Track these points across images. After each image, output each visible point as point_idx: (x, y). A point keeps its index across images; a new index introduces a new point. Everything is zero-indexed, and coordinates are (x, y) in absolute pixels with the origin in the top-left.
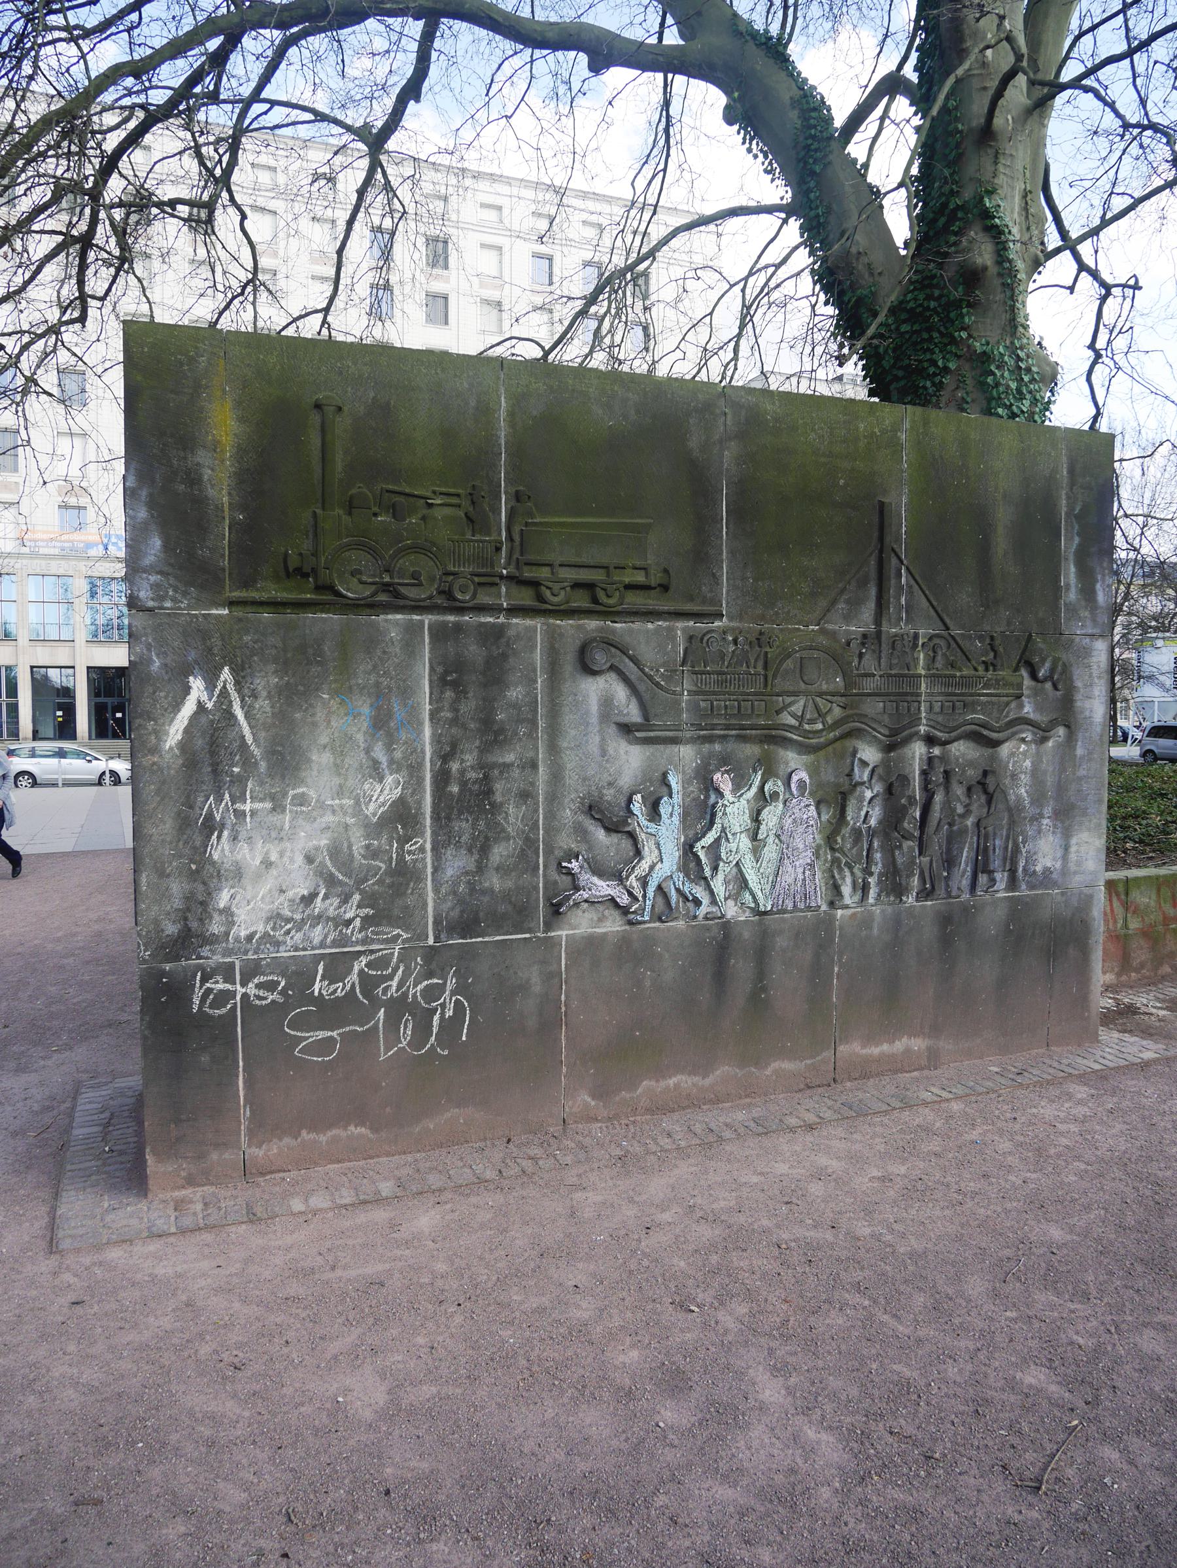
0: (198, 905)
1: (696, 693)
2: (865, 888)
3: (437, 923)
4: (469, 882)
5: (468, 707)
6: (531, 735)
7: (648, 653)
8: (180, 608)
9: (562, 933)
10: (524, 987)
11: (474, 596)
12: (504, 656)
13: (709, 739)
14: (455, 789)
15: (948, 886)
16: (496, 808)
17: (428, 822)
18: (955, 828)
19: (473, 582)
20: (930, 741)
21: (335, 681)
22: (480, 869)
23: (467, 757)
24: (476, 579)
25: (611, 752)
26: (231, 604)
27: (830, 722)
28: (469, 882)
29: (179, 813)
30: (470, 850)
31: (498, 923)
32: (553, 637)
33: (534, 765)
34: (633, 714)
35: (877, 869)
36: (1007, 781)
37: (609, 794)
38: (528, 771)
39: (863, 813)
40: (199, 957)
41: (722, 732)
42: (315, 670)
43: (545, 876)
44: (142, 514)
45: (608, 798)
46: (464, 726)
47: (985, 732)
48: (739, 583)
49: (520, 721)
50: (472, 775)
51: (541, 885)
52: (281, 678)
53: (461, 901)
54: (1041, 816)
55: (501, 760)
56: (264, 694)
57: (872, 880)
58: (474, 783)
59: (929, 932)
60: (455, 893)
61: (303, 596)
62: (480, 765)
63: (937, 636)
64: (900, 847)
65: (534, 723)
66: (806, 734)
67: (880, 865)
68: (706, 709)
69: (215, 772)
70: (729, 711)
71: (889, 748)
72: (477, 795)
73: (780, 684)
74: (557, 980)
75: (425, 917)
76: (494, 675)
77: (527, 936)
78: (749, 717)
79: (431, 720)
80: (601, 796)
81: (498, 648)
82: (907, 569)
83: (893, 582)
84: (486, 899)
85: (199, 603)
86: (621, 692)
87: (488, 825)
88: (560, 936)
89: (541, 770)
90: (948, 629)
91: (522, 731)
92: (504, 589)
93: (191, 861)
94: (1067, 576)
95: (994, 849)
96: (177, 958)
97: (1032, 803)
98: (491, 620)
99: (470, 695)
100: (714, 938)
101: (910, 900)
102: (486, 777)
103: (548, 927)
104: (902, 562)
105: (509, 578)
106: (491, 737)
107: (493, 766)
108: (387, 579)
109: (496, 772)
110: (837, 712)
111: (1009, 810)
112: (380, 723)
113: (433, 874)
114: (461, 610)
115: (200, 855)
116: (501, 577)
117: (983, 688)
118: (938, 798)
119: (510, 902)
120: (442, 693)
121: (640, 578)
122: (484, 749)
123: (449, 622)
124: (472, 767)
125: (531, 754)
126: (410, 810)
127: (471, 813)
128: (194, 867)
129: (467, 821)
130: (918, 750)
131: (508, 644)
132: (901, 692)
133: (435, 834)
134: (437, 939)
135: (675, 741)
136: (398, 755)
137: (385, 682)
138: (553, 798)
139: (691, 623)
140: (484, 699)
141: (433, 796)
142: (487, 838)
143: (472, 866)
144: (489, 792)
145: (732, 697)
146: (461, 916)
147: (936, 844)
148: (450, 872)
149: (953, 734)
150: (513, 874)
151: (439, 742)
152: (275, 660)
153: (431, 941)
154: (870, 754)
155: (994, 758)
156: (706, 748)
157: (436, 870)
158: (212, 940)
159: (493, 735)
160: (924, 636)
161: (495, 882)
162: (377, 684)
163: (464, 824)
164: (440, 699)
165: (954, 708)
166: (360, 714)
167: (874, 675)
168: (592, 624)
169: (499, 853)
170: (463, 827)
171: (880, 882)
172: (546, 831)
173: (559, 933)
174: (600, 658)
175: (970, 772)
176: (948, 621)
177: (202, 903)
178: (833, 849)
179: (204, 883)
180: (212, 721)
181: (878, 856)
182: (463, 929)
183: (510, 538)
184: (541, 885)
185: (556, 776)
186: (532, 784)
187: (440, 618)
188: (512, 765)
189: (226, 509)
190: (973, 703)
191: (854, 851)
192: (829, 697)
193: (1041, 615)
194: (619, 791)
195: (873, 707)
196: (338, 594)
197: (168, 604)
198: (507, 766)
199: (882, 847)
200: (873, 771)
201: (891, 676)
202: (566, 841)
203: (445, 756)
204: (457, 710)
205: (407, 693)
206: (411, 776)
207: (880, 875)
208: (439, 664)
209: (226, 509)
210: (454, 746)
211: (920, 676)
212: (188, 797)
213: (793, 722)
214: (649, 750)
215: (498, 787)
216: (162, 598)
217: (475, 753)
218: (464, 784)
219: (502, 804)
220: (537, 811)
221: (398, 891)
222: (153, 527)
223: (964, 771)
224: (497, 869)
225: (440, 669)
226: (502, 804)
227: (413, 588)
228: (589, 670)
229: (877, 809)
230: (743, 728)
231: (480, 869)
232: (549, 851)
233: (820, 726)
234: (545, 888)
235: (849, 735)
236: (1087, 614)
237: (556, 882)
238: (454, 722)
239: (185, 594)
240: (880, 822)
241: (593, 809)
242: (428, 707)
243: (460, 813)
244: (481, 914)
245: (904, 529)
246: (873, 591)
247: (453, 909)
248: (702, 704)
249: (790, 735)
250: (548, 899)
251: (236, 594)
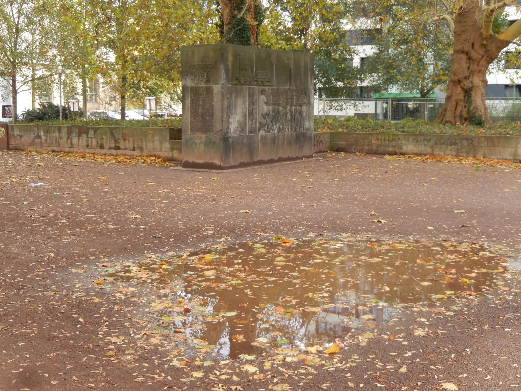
0: (228, 128)
5: (251, 100)
7: (267, 91)
32: (259, 89)
34: (266, 101)
62: (252, 108)
76: (253, 96)
86: (265, 97)
112: (244, 102)
115: (228, 120)
132: (292, 99)
147: (296, 122)
159: (253, 104)
168: (262, 87)
169: (254, 121)
174: (264, 92)
185: (259, 110)
202: (260, 120)
203: (249, 107)
205: (246, 97)
228: (262, 94)
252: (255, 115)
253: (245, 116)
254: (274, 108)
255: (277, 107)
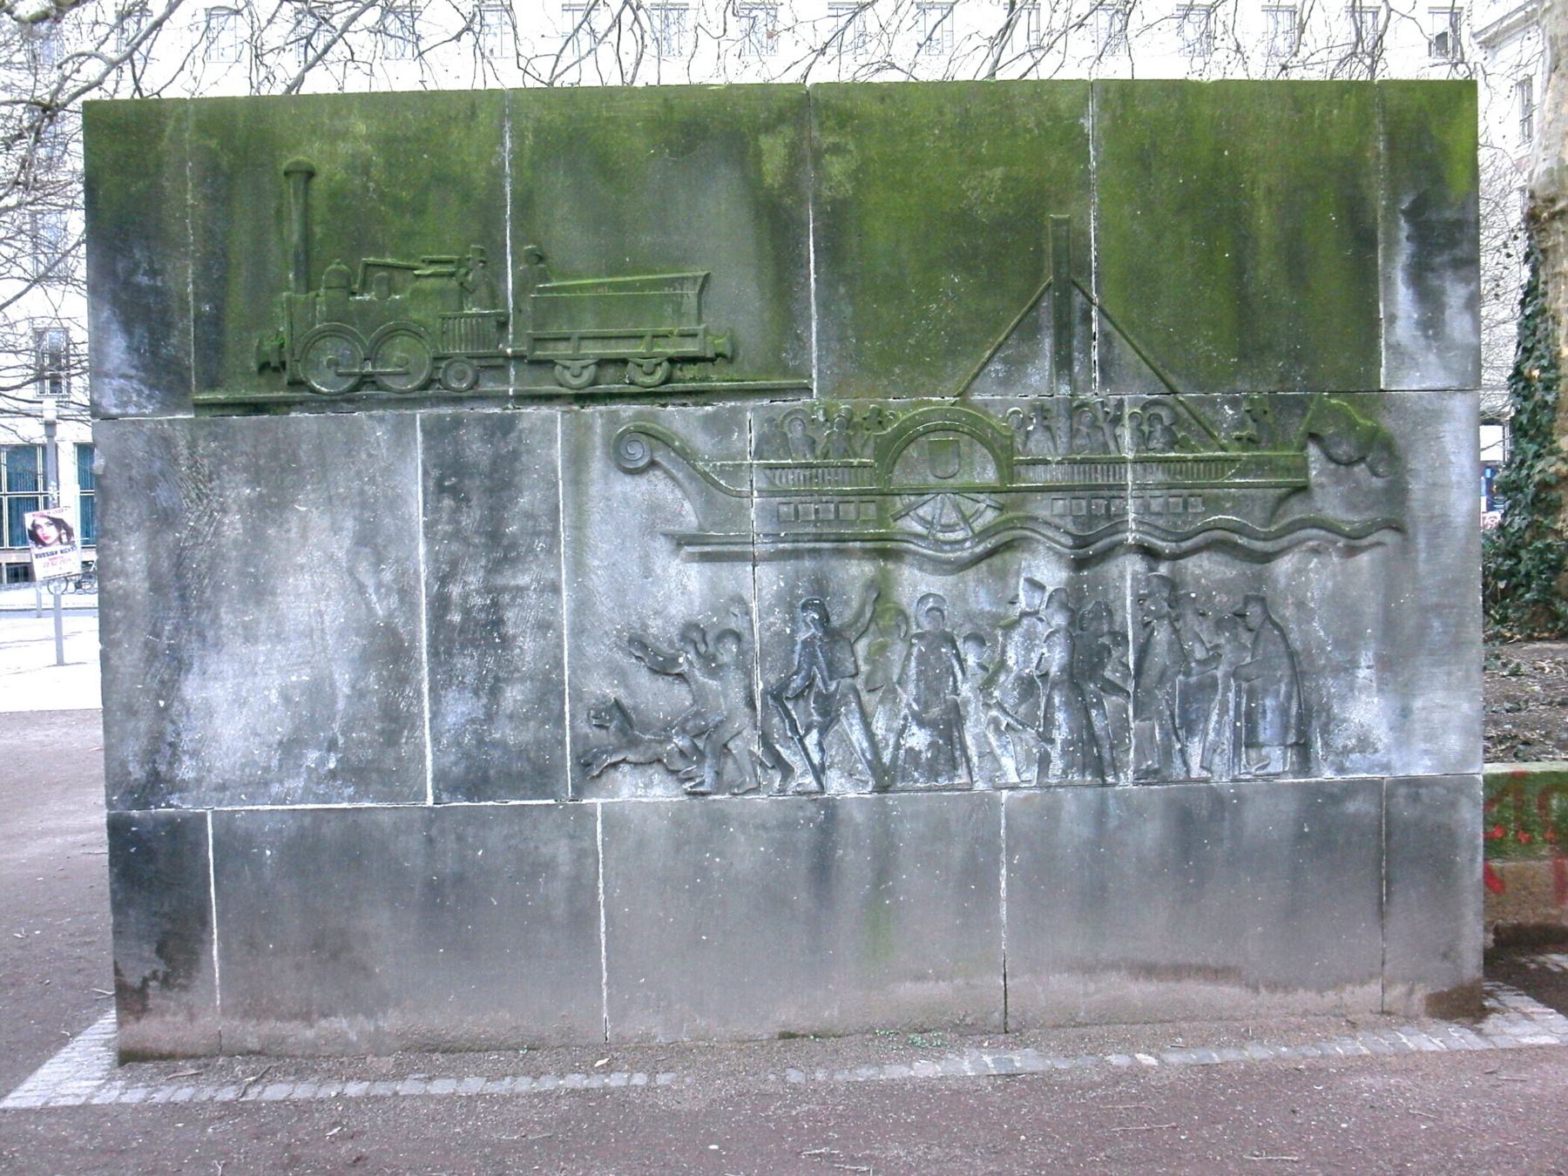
1: (773, 494)
2: (1044, 762)
3: (436, 780)
4: (475, 732)
5: (470, 519)
6: (552, 550)
8: (144, 415)
9: (596, 802)
10: (549, 865)
11: (476, 383)
12: (515, 455)
13: (796, 554)
14: (456, 618)
15: (1185, 763)
16: (506, 642)
17: (425, 657)
18: (1193, 679)
19: (471, 365)
20: (1150, 554)
21: (314, 491)
22: (490, 717)
23: (471, 579)
24: (475, 362)
25: (659, 571)
26: (199, 406)
27: (977, 529)
28: (475, 732)
29: (146, 644)
30: (476, 692)
31: (514, 783)
33: (555, 589)
35: (1060, 735)
36: (1289, 612)
37: (655, 626)
38: (548, 596)
39: (1035, 657)
40: (171, 806)
41: (811, 545)
42: (290, 479)
43: (572, 728)
44: (106, 314)
45: (653, 631)
46: (465, 541)
47: (1242, 541)
48: (836, 346)
49: (538, 534)
50: (477, 601)
51: (568, 739)
52: (253, 489)
53: (467, 755)
54: (1354, 665)
55: (513, 583)
56: (235, 508)
57: (1055, 752)
58: (480, 610)
59: (1152, 833)
60: (459, 744)
61: (275, 394)
62: (488, 589)
63: (1155, 403)
64: (1100, 705)
65: (554, 534)
66: (938, 545)
67: (1065, 729)
68: (788, 515)
69: (183, 597)
70: (821, 516)
71: (1079, 564)
72: (485, 626)
73: (899, 477)
74: (591, 860)
75: (423, 772)
76: (501, 481)
77: (552, 802)
78: (852, 523)
79: (426, 535)
80: (645, 627)
81: (507, 444)
82: (1101, 310)
83: (1079, 329)
84: (496, 754)
85: (166, 408)
87: (497, 662)
88: (594, 805)
89: (565, 593)
90: (1173, 391)
91: (539, 545)
92: (512, 372)
93: (160, 697)
94: (1390, 302)
95: (1264, 712)
96: (145, 805)
97: (1337, 644)
98: (498, 410)
99: (474, 502)
100: (811, 820)
101: (1126, 780)
102: (495, 604)
103: (579, 791)
104: (1090, 300)
105: (518, 357)
106: (499, 554)
107: (504, 589)
108: (369, 368)
109: (507, 597)
110: (990, 516)
111: (1292, 655)
113: (431, 720)
114: (457, 400)
116: (507, 357)
117: (1234, 476)
118: (1161, 635)
119: (529, 759)
120: (439, 501)
121: (691, 348)
122: (495, 568)
123: (445, 416)
124: (478, 592)
125: (552, 575)
126: (402, 641)
127: (477, 647)
128: (162, 703)
129: (472, 657)
130: (1132, 566)
131: (520, 440)
133: (432, 672)
134: (437, 800)
135: (740, 557)
136: (387, 576)
137: (370, 490)
138: (578, 631)
139: (766, 402)
140: (491, 509)
141: (429, 626)
142: (497, 679)
143: (481, 714)
144: (499, 623)
145: (824, 499)
146: (468, 773)
148: (451, 719)
149: (1185, 545)
150: (532, 723)
151: (436, 561)
152: (246, 469)
153: (430, 802)
154: (1051, 573)
155: (1259, 579)
156: (790, 566)
157: (435, 715)
158: (181, 787)
159: (502, 551)
160: (1134, 403)
161: (505, 732)
162: (362, 493)
163: (468, 661)
164: (437, 510)
165: (1185, 506)
166: (342, 529)
167: (1046, 463)
169: (514, 695)
170: (466, 663)
171: (1064, 753)
172: (573, 672)
173: (594, 800)
175: (1220, 598)
176: (1173, 380)
177: (171, 744)
178: (987, 706)
179: (173, 722)
180: (179, 540)
181: (1060, 717)
182: (469, 789)
183: (518, 310)
184: (568, 739)
185: (583, 606)
186: (553, 612)
187: (435, 411)
188: (527, 588)
189: (191, 298)
190: (1217, 499)
191: (1022, 709)
192: (973, 496)
193: (1342, 363)
194: (669, 620)
195: (1047, 508)
196: (313, 390)
197: (132, 410)
198: (520, 590)
199: (1067, 704)
200: (1051, 596)
201: (1073, 462)
204: (458, 522)
206: (402, 601)
207: (1066, 743)
208: (435, 466)
209: (191, 298)
210: (454, 564)
211: (1124, 461)
212: (155, 625)
213: (919, 529)
214: (708, 569)
215: (510, 615)
216: (124, 404)
217: (481, 574)
218: (467, 612)
219: (515, 637)
220: (560, 646)
221: (391, 739)
222: (115, 327)
223: (1210, 597)
224: (511, 717)
225: (435, 473)
226: (515, 637)
227: (397, 379)
229: (1058, 649)
230: (841, 539)
231: (490, 717)
232: (577, 696)
233: (959, 535)
234: (573, 742)
235: (1008, 546)
236: (1432, 358)
237: (586, 736)
238: (457, 535)
239: (150, 397)
240: (1062, 670)
241: (638, 644)
242: (421, 519)
243: (463, 647)
244: (492, 772)
245: (1094, 253)
246: (1047, 344)
247: (456, 764)
248: (784, 509)
249: (911, 546)
250: (577, 758)
251: (205, 396)
252: (527, 646)
253: (388, 650)
254: (820, 586)
255: (856, 572)
